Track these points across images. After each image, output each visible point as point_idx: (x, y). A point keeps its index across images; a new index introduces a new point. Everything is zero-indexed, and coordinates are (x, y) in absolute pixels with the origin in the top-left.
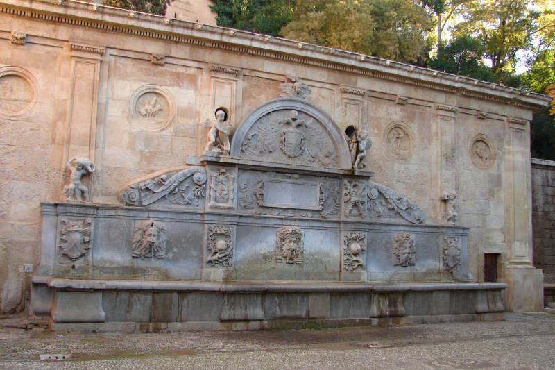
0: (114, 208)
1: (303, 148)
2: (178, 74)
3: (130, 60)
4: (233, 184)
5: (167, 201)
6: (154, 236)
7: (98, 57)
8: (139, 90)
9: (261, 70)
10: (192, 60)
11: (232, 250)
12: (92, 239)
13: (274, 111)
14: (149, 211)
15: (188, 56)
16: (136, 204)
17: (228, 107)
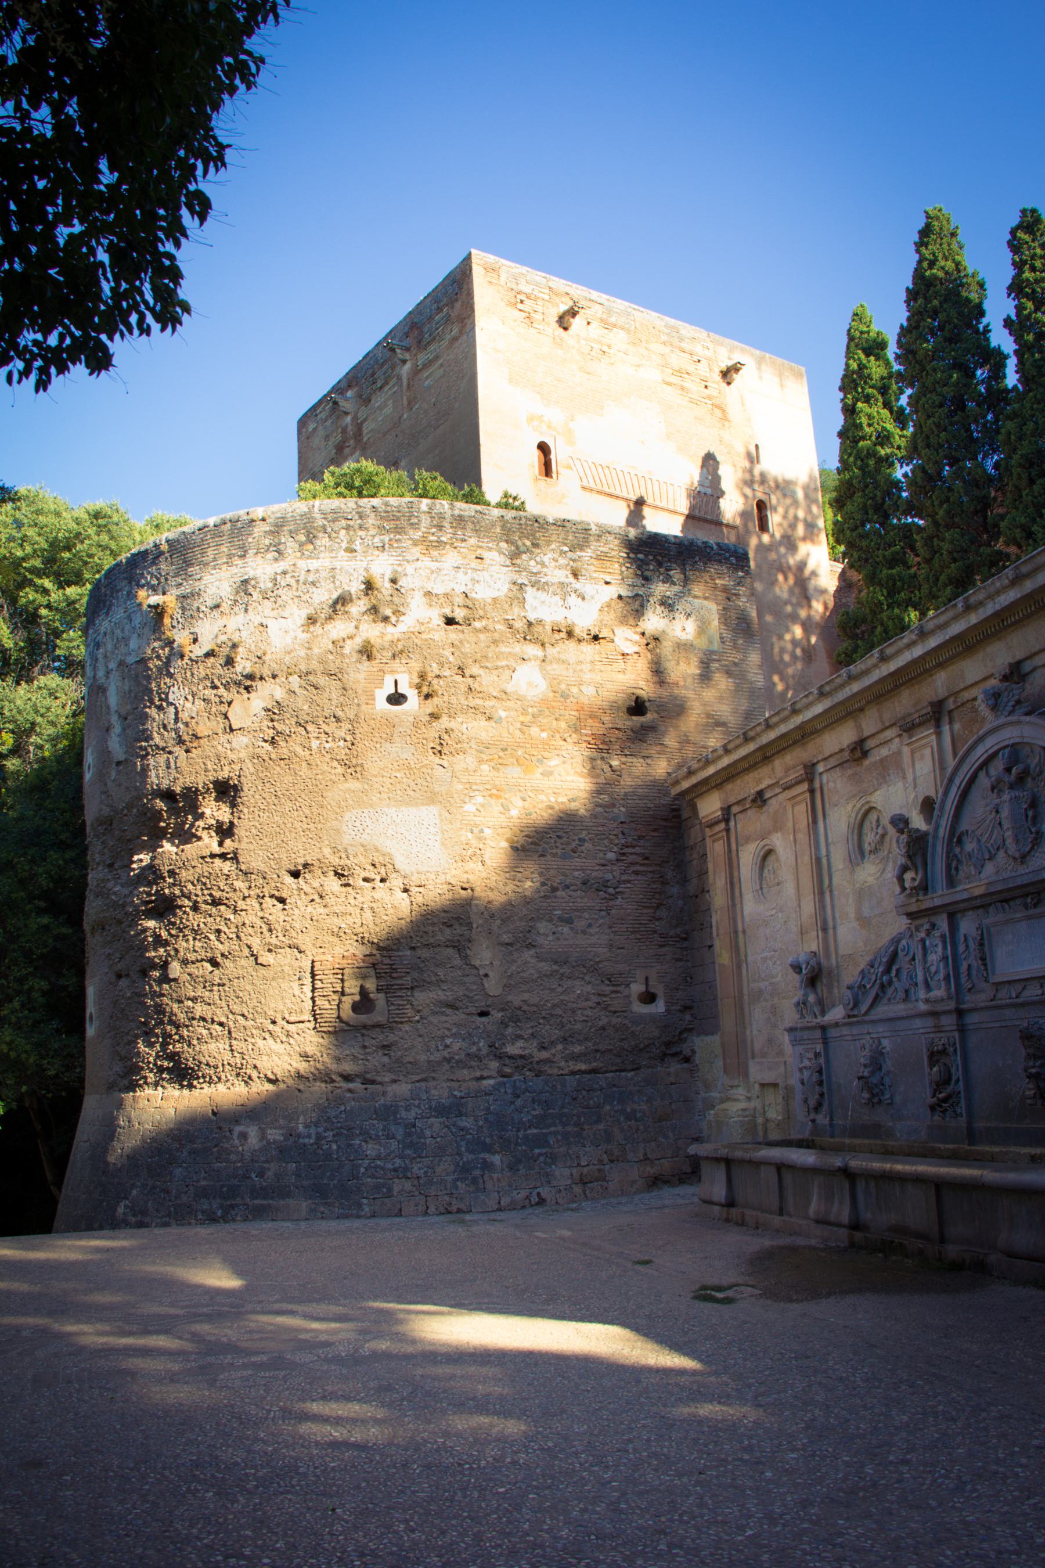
0: (837, 1025)
1: (1033, 830)
2: (881, 761)
3: (837, 769)
4: (945, 948)
5: (885, 1001)
6: (865, 1066)
7: (805, 786)
8: (853, 815)
9: (962, 686)
10: (887, 728)
11: (958, 1081)
12: (824, 1077)
13: (980, 768)
14: (866, 1022)
15: (879, 727)
16: (855, 1012)
17: (932, 793)
